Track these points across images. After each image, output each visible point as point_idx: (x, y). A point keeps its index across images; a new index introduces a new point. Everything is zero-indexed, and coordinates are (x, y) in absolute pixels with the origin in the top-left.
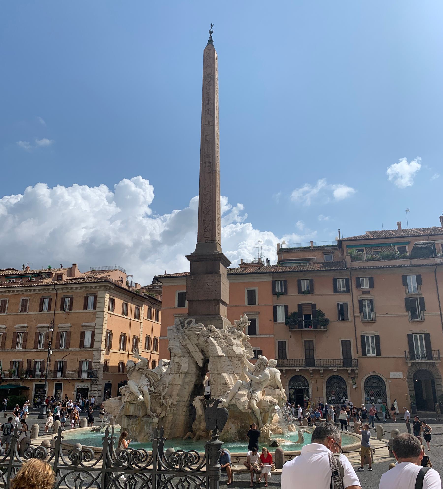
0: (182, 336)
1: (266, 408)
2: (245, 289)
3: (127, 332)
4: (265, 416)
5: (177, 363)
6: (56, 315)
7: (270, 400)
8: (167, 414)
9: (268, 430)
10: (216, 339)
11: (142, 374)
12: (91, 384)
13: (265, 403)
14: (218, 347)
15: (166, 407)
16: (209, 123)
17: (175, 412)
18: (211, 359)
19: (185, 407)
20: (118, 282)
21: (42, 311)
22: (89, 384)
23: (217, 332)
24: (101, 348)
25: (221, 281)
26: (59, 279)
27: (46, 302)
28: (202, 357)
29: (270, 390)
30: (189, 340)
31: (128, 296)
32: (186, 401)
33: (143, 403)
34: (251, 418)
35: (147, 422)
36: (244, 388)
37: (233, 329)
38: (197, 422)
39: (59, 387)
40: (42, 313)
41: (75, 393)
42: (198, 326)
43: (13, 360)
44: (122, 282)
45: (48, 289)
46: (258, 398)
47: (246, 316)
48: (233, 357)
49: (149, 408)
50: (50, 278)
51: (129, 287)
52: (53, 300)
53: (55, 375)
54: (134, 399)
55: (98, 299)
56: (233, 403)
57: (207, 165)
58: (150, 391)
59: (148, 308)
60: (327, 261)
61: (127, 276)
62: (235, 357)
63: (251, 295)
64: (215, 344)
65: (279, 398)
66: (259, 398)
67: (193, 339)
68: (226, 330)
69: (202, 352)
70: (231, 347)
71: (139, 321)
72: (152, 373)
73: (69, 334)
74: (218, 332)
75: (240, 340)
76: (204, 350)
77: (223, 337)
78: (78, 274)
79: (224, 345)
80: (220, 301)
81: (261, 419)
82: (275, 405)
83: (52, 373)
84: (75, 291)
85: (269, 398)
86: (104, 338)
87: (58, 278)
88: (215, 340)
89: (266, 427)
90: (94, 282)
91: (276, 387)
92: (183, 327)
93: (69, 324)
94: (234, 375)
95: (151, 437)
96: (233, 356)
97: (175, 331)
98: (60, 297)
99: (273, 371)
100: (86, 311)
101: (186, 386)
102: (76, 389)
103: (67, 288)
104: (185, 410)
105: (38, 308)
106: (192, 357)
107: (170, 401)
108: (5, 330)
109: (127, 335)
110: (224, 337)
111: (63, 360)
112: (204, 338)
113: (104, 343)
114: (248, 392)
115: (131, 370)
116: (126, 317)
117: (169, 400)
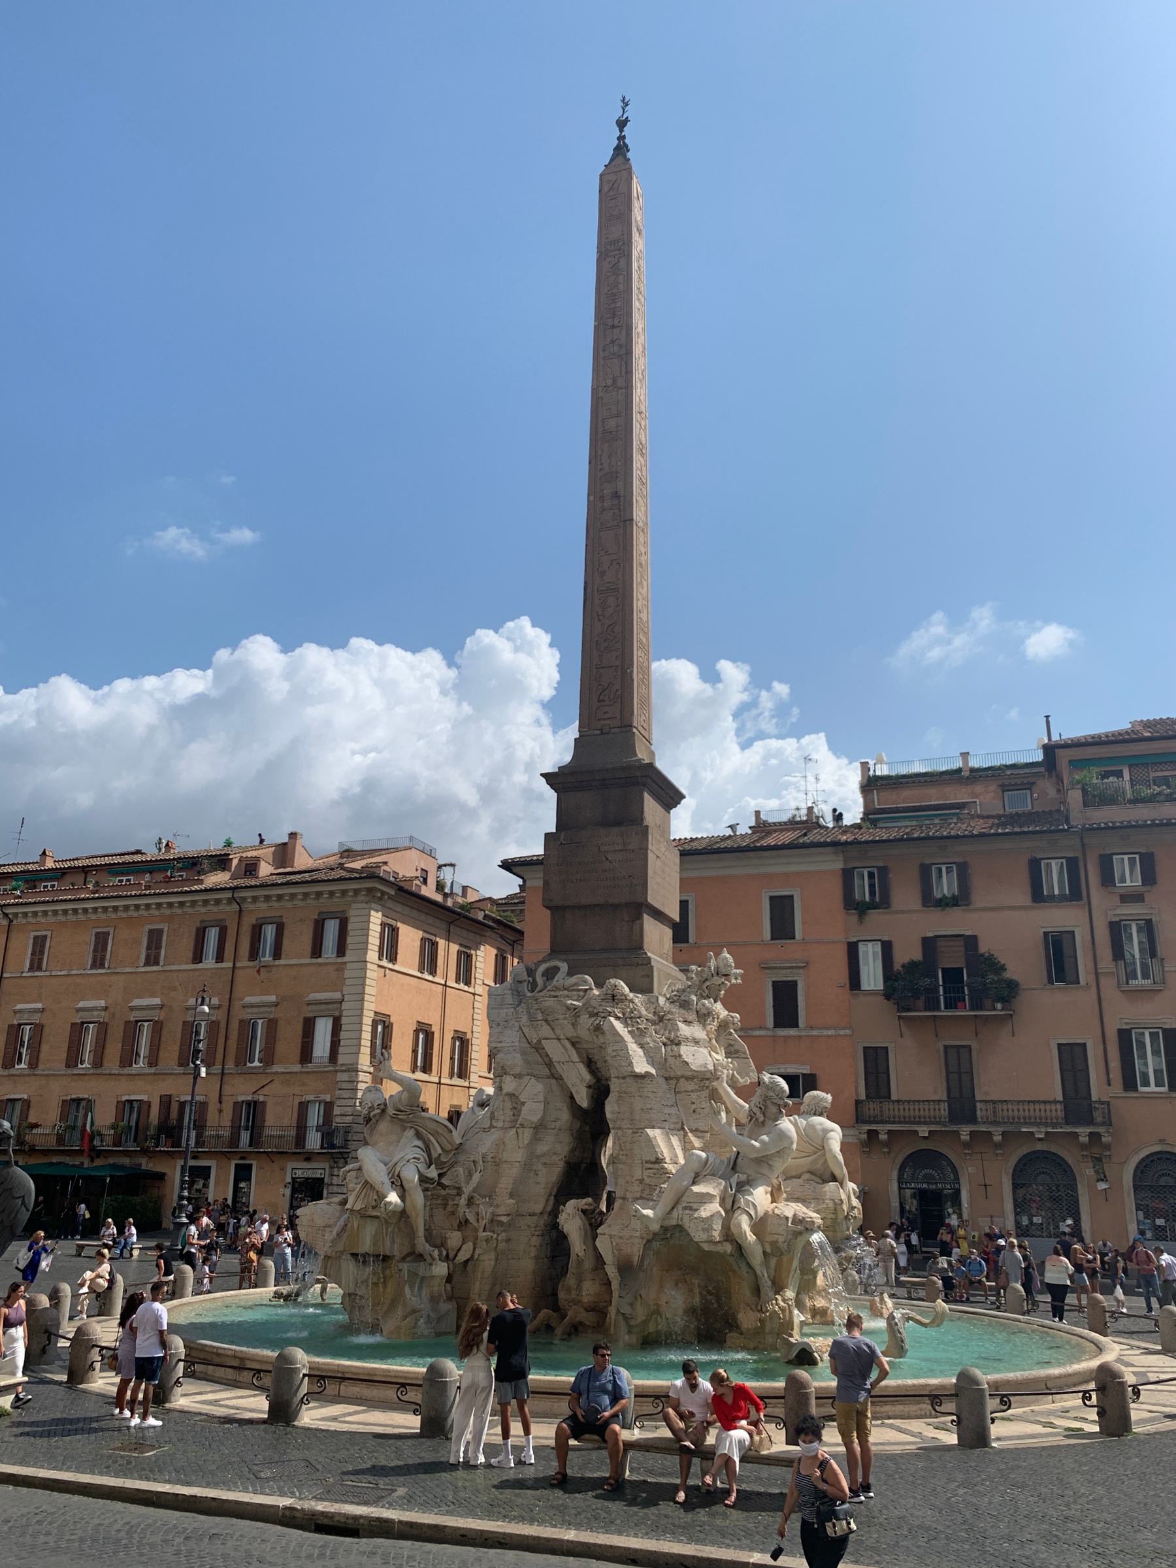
0: (529, 1013)
1: (781, 1239)
2: (763, 894)
3: (433, 1019)
4: (779, 1263)
5: (511, 1095)
6: (238, 973)
7: (795, 1215)
8: (477, 1252)
9: (791, 1313)
10: (629, 1022)
11: (404, 1129)
12: (332, 1168)
13: (779, 1225)
14: (633, 1048)
15: (476, 1230)
16: (614, 381)
17: (502, 1246)
18: (615, 1085)
19: (536, 1233)
20: (411, 880)
21: (201, 962)
22: (326, 1165)
23: (631, 1001)
24: (357, 1064)
25: (647, 849)
26: (251, 874)
27: (213, 935)
28: (587, 1077)
29: (807, 1186)
30: (549, 1025)
31: (438, 918)
32: (541, 1213)
33: (403, 1215)
34: (734, 1271)
35: (413, 1274)
36: (713, 1175)
37: (686, 994)
38: (570, 1280)
39: (243, 1173)
40: (200, 966)
41: (288, 1192)
42: (575, 984)
43: (124, 1098)
44: (425, 881)
45: (218, 902)
46: (754, 1205)
47: (726, 954)
48: (682, 1080)
49: (421, 1232)
50: (224, 870)
51: (446, 896)
52: (229, 931)
53: (234, 1140)
54: (374, 1203)
55: (350, 926)
56: (674, 1223)
57: (607, 504)
58: (423, 1179)
59: (496, 955)
60: (1014, 811)
61: (440, 867)
62: (687, 1079)
63: (782, 910)
64: (626, 1039)
65: (835, 1209)
66: (759, 1209)
67: (561, 1021)
68: (665, 995)
69: (590, 1064)
70: (675, 1048)
71: (471, 990)
72: (435, 1124)
73: (272, 1025)
74: (636, 1001)
75: (708, 1028)
76: (596, 1057)
77: (651, 1016)
78: (302, 861)
79: (654, 1041)
80: (644, 908)
81: (766, 1275)
82: (812, 1230)
83: (226, 1133)
84: (288, 904)
85: (790, 1209)
86: (366, 1035)
87: (246, 872)
88: (626, 1025)
89: (784, 1300)
90: (340, 879)
91: (827, 1176)
92: (533, 986)
93: (273, 998)
94: (685, 1135)
95: (422, 1321)
96: (683, 1076)
97: (509, 999)
98: (249, 921)
99: (819, 1127)
100: (319, 960)
101: (540, 1167)
102: (289, 1179)
103: (267, 898)
104: (535, 1241)
105: (190, 955)
106: (559, 1079)
107: (485, 1211)
108: (103, 1013)
109: (436, 1029)
110: (655, 1018)
111: (256, 1097)
112: (593, 1019)
113: (365, 1050)
114: (722, 1188)
115: (372, 1114)
116: (430, 978)
117: (482, 1209)
